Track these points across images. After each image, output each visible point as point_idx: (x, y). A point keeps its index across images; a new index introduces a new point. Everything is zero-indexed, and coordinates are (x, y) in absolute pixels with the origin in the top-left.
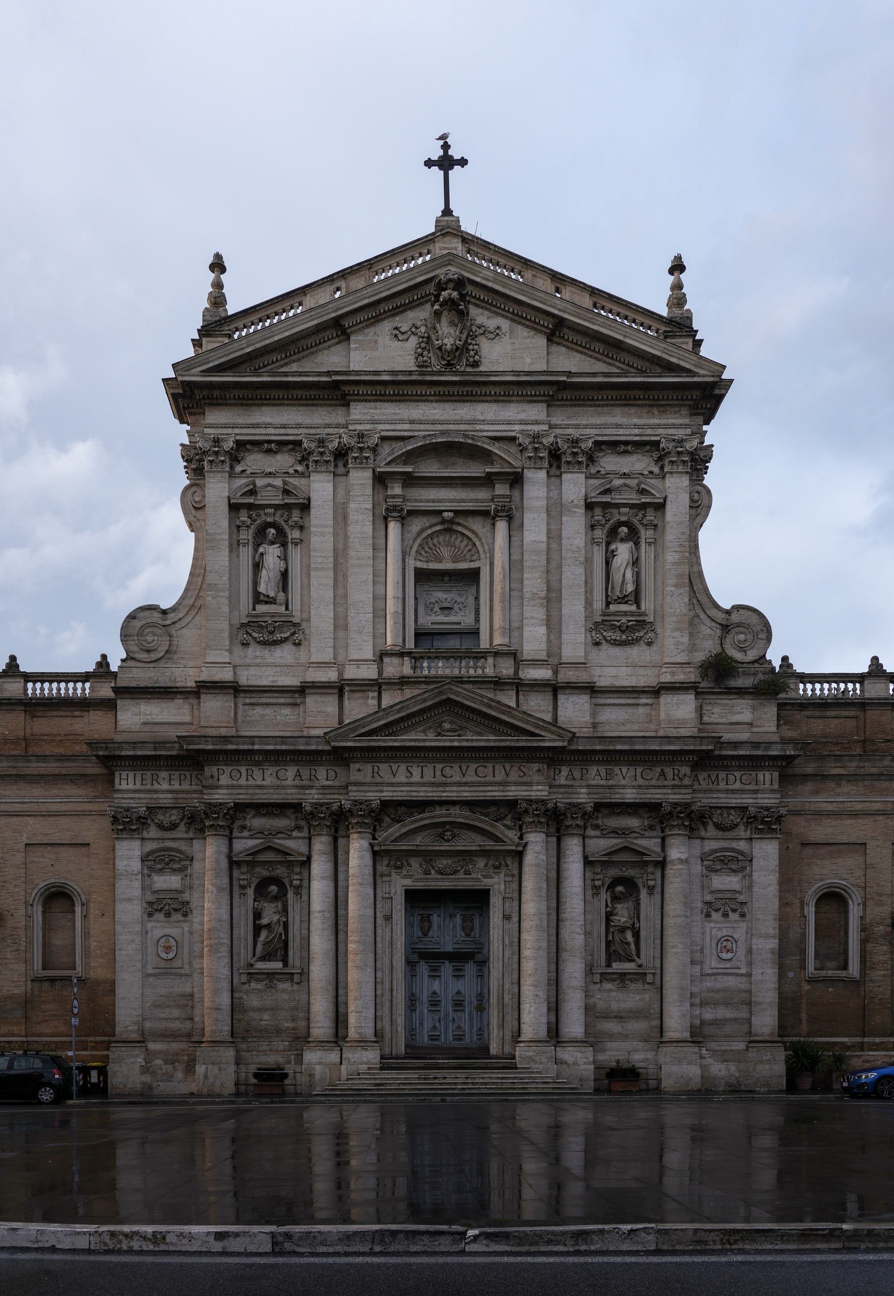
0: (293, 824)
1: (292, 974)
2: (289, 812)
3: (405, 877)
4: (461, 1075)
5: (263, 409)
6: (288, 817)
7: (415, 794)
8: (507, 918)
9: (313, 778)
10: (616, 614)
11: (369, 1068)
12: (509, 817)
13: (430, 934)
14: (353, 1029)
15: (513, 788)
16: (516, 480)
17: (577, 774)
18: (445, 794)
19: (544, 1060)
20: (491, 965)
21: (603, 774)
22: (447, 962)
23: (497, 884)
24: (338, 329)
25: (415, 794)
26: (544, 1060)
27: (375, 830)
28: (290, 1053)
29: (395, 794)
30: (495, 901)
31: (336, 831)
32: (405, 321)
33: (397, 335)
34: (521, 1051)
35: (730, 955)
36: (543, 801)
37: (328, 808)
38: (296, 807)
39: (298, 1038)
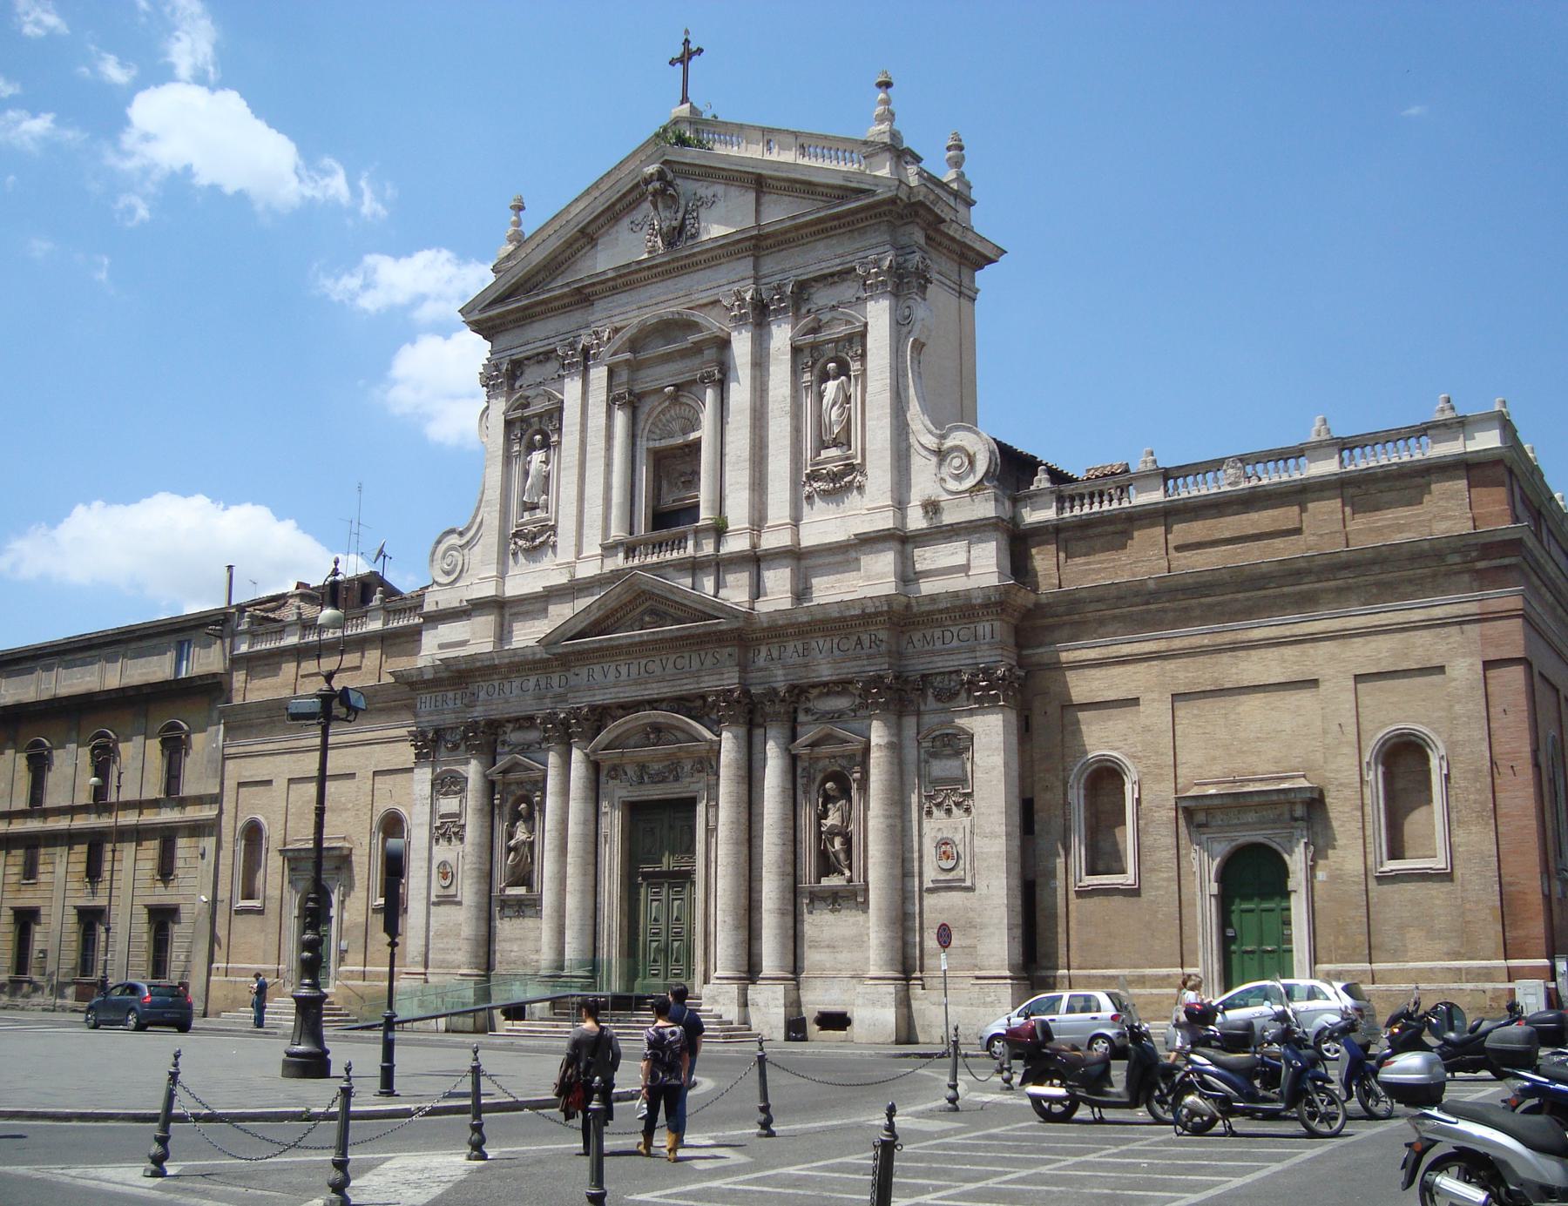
5: (536, 325)
10: (826, 461)
16: (724, 344)
24: (587, 236)
32: (638, 215)
33: (635, 227)
35: (951, 863)
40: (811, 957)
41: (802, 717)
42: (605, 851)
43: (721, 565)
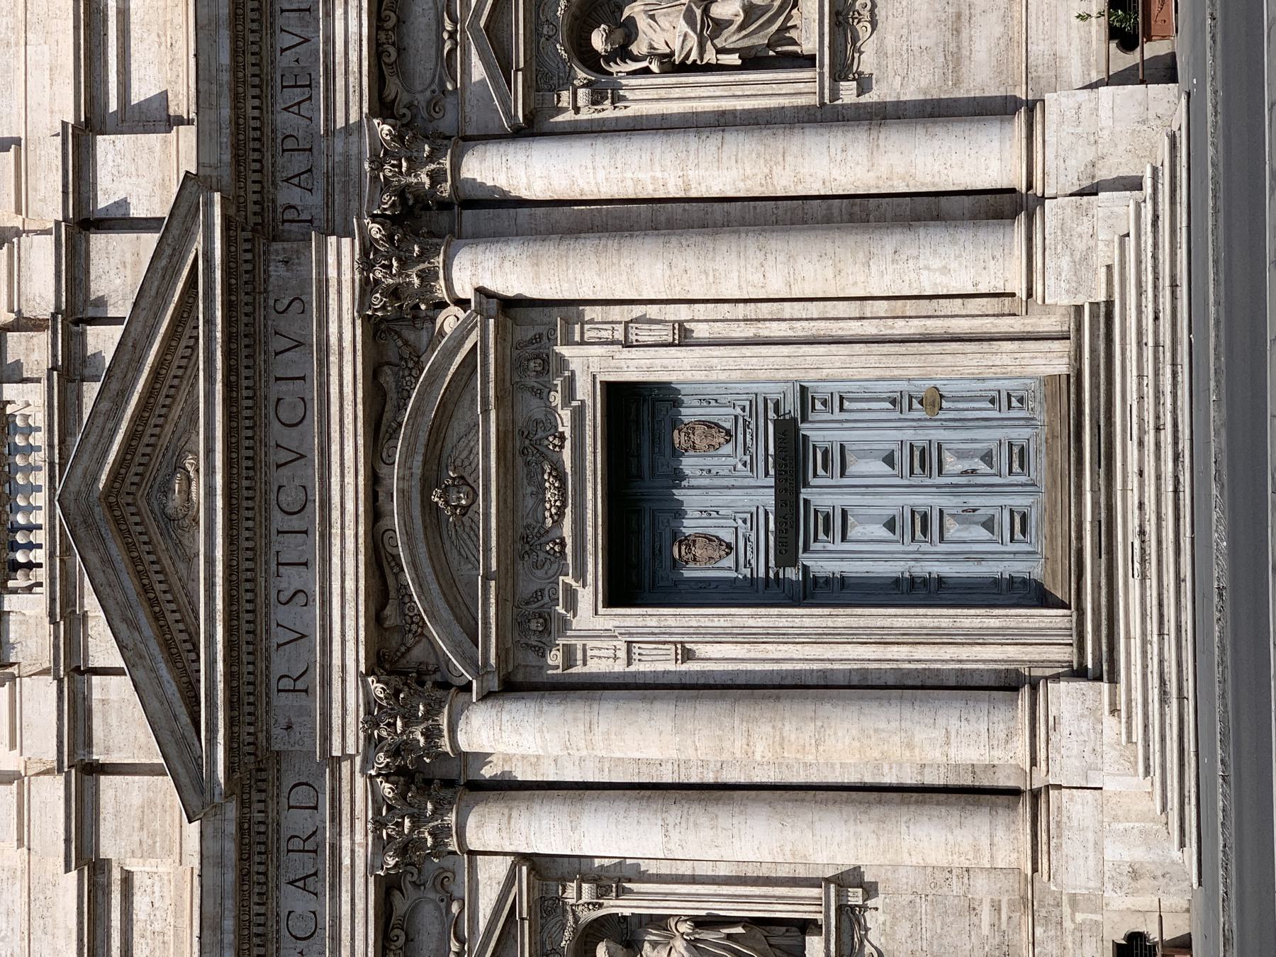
0: (432, 895)
1: (840, 908)
2: (401, 905)
3: (572, 604)
4: (1128, 456)
6: (414, 909)
7: (350, 585)
8: (683, 337)
9: (310, 845)
11: (1114, 711)
12: (411, 336)
13: (728, 536)
14: (998, 753)
15: (333, 328)
17: (298, 163)
18: (350, 506)
19: (1085, 227)
20: (813, 375)
21: (297, 95)
22: (805, 493)
23: (591, 364)
25: (350, 585)
26: (1085, 227)
27: (445, 685)
28: (1068, 924)
29: (350, 634)
30: (634, 367)
31: (449, 783)
34: (1061, 291)
36: (365, 252)
37: (390, 808)
38: (387, 888)
39: (1023, 898)
40: (980, 80)
41: (447, 123)
42: (718, 657)
43: (77, 310)
